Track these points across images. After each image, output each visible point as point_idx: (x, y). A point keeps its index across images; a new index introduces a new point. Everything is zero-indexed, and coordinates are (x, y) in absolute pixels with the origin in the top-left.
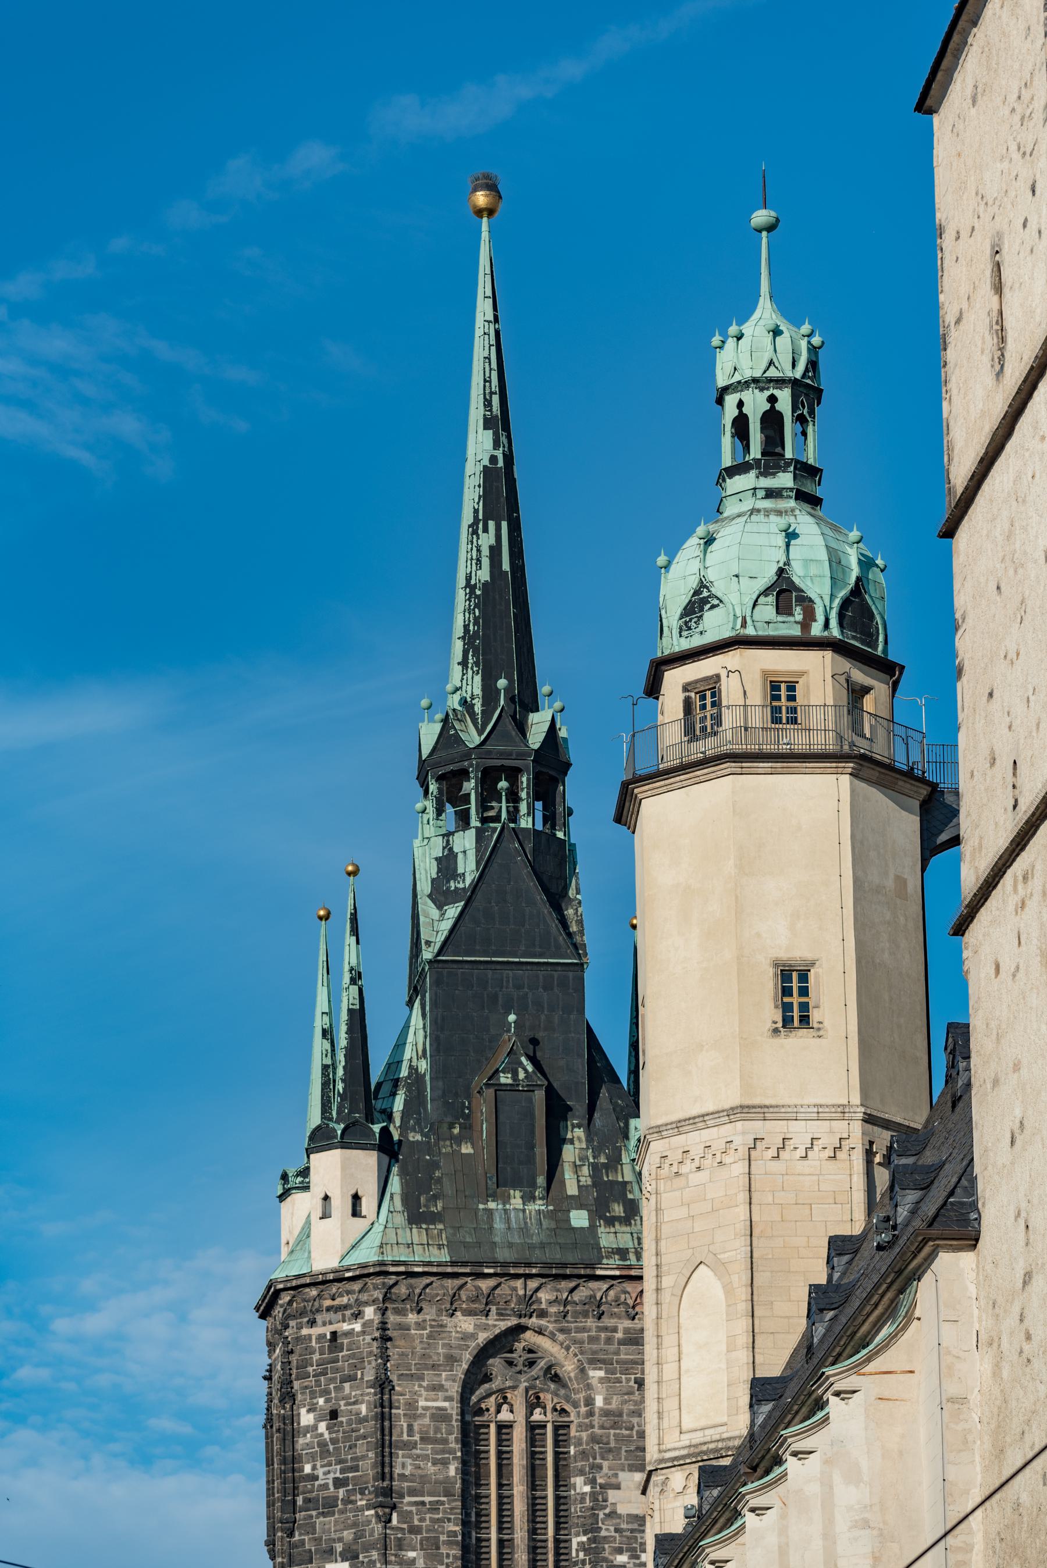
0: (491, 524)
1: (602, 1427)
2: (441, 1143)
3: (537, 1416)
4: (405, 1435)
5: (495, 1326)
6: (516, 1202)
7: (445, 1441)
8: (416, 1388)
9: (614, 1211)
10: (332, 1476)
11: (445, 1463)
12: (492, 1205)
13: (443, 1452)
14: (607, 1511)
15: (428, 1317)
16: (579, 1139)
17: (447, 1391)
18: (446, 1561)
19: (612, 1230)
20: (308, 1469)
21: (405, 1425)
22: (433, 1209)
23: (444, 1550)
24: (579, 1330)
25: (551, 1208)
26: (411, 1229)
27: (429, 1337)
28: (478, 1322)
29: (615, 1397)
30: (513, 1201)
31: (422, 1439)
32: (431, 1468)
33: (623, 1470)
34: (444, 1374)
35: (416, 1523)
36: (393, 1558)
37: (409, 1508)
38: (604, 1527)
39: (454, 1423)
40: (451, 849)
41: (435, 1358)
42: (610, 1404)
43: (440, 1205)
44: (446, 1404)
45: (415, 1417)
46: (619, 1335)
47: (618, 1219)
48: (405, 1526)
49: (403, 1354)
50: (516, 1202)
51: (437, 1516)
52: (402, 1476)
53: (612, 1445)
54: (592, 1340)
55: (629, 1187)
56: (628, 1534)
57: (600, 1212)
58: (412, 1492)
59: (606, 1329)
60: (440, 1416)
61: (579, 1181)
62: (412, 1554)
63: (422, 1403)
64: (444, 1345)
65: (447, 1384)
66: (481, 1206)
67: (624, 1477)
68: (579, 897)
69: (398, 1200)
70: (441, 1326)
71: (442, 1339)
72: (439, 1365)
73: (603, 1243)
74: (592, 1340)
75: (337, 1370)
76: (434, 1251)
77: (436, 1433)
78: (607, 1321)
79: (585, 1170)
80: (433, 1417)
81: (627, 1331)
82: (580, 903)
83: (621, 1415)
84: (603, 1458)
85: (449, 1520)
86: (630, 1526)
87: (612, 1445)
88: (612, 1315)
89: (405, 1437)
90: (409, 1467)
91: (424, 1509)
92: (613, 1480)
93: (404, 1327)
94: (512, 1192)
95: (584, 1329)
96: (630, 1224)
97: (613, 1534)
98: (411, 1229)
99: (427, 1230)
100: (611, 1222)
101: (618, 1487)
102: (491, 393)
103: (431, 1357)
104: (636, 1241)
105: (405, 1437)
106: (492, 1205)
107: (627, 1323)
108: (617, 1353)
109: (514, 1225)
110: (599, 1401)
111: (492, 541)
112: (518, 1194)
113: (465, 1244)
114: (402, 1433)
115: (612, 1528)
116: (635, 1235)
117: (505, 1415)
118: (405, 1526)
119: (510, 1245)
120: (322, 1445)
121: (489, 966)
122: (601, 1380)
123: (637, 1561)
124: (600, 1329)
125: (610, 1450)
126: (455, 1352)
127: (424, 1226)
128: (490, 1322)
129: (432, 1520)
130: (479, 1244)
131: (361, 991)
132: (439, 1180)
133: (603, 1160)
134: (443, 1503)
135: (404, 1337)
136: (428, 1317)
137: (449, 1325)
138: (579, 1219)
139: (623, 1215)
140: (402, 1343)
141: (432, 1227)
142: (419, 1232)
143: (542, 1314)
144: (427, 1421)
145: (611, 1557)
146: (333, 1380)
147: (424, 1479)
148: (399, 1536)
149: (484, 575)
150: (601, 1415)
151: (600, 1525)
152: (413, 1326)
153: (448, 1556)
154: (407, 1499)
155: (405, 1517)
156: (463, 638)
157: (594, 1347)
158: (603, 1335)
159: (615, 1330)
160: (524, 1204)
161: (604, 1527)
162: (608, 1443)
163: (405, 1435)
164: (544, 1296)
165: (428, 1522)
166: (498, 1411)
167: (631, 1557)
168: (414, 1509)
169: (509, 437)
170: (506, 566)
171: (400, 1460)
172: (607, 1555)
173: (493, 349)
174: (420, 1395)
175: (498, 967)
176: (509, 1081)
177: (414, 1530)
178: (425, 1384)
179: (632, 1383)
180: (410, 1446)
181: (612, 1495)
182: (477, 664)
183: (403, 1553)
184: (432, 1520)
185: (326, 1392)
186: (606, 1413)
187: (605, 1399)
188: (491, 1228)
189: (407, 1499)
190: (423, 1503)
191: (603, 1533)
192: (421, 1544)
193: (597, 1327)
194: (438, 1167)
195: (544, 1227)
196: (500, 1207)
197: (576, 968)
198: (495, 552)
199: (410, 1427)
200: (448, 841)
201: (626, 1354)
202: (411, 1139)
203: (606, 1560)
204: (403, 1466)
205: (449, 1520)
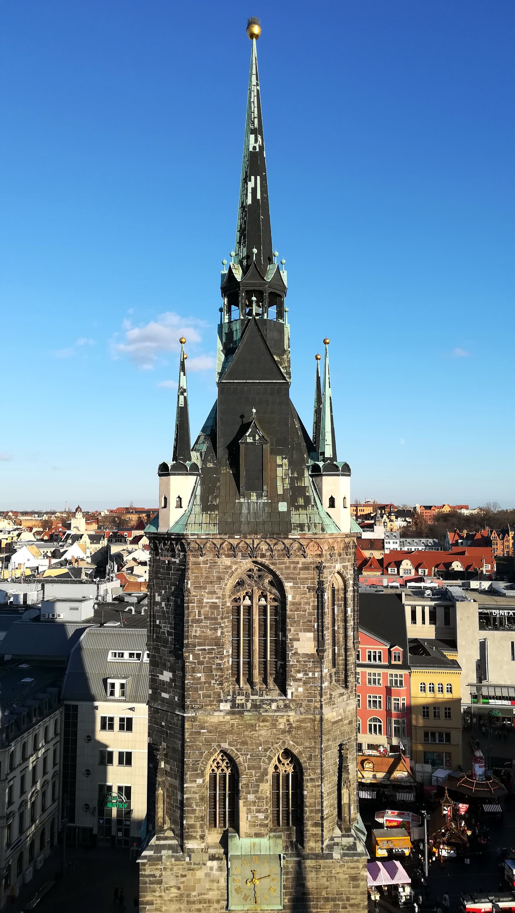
0: (253, 178)
1: (291, 611)
2: (222, 468)
3: (263, 602)
4: (197, 616)
5: (241, 562)
6: (254, 498)
7: (216, 619)
8: (203, 593)
9: (299, 502)
10: (166, 629)
11: (216, 629)
12: (242, 500)
13: (216, 624)
14: (293, 652)
15: (209, 559)
16: (285, 464)
17: (217, 594)
18: (215, 678)
19: (298, 513)
20: (158, 622)
21: (197, 611)
22: (214, 503)
23: (214, 673)
24: (281, 563)
25: (270, 501)
26: (203, 514)
27: (209, 568)
28: (232, 560)
29: (297, 596)
30: (252, 498)
31: (205, 618)
32: (209, 632)
33: (301, 632)
34: (216, 586)
35: (201, 659)
36: (190, 677)
37: (198, 652)
38: (291, 660)
39: (220, 610)
40: (231, 329)
41: (212, 578)
42: (295, 599)
43: (218, 500)
44: (217, 601)
45: (202, 607)
46: (300, 565)
47: (301, 506)
48: (196, 661)
49: (196, 577)
50: (254, 498)
51: (211, 656)
52: (195, 636)
53: (296, 619)
54: (287, 568)
55: (307, 489)
56: (303, 663)
57: (292, 504)
58: (200, 644)
59: (294, 562)
60: (214, 606)
61: (283, 487)
62: (199, 675)
63: (205, 600)
64: (216, 572)
65: (218, 591)
66: (237, 501)
67: (301, 635)
68: (289, 349)
69: (198, 498)
70: (215, 563)
71: (215, 569)
72: (214, 582)
73: (293, 521)
74: (287, 568)
75: (170, 579)
76: (212, 526)
77: (211, 615)
78: (294, 559)
79: (287, 481)
80: (211, 607)
81: (303, 563)
82: (289, 352)
83: (300, 604)
84: (291, 626)
85: (217, 658)
86: (304, 659)
87: (296, 619)
88: (297, 556)
89: (197, 617)
90: (199, 632)
91: (205, 652)
92: (296, 637)
93: (197, 564)
94: (252, 493)
95: (283, 563)
96: (307, 509)
97: (296, 663)
98: (203, 514)
99: (210, 514)
100: (297, 508)
101: (298, 640)
102: (254, 118)
103: (210, 578)
104: (309, 519)
105: (197, 617)
106: (242, 500)
107: (303, 560)
108: (299, 574)
109: (252, 511)
110: (290, 598)
111: (253, 186)
112: (255, 494)
113: (227, 523)
114: (195, 615)
115: (295, 661)
116: (308, 515)
117: (247, 602)
118: (196, 661)
119: (249, 523)
120: (163, 612)
121: (245, 385)
122: (291, 587)
123: (307, 677)
124: (291, 563)
125: (295, 622)
126: (221, 575)
127: (209, 513)
128: (238, 560)
129: (209, 658)
130: (233, 523)
131: (185, 398)
132: (219, 488)
133: (296, 475)
134: (214, 649)
135: (198, 568)
136: (209, 559)
137: (219, 562)
138: (283, 507)
139: (303, 504)
140: (196, 571)
141: (213, 513)
142: (206, 516)
143: (263, 556)
144: (207, 609)
145: (294, 675)
146: (168, 583)
147: (206, 638)
148: (193, 666)
149: (249, 201)
150: (290, 605)
151: (290, 659)
152: (202, 563)
153: (216, 675)
154: (197, 648)
155: (196, 656)
156: (239, 231)
157: (288, 571)
158: (292, 566)
159: (298, 563)
160: (257, 500)
161: (291, 660)
162: (294, 618)
163: (197, 616)
164: (264, 547)
165: (207, 659)
166: (244, 600)
167: (305, 675)
168: (200, 652)
169: (262, 138)
170: (259, 197)
171: (194, 628)
172: (293, 674)
173: (256, 98)
174: (205, 597)
175: (249, 385)
176: (252, 441)
177: (201, 663)
178: (207, 591)
179: (306, 589)
180: (199, 621)
181: (296, 644)
182: (244, 243)
183: (195, 674)
184: (209, 658)
185: (165, 588)
186: (293, 604)
187: (293, 597)
188: (241, 513)
189: (197, 648)
190: (205, 650)
191: (291, 663)
192: (204, 670)
193: (289, 562)
194: (219, 481)
195: (266, 512)
196: (246, 501)
197: (285, 384)
198: (254, 190)
199: (199, 612)
200: (230, 325)
201: (303, 575)
202: (208, 466)
203: (292, 676)
204: (196, 631)
205: (217, 658)
